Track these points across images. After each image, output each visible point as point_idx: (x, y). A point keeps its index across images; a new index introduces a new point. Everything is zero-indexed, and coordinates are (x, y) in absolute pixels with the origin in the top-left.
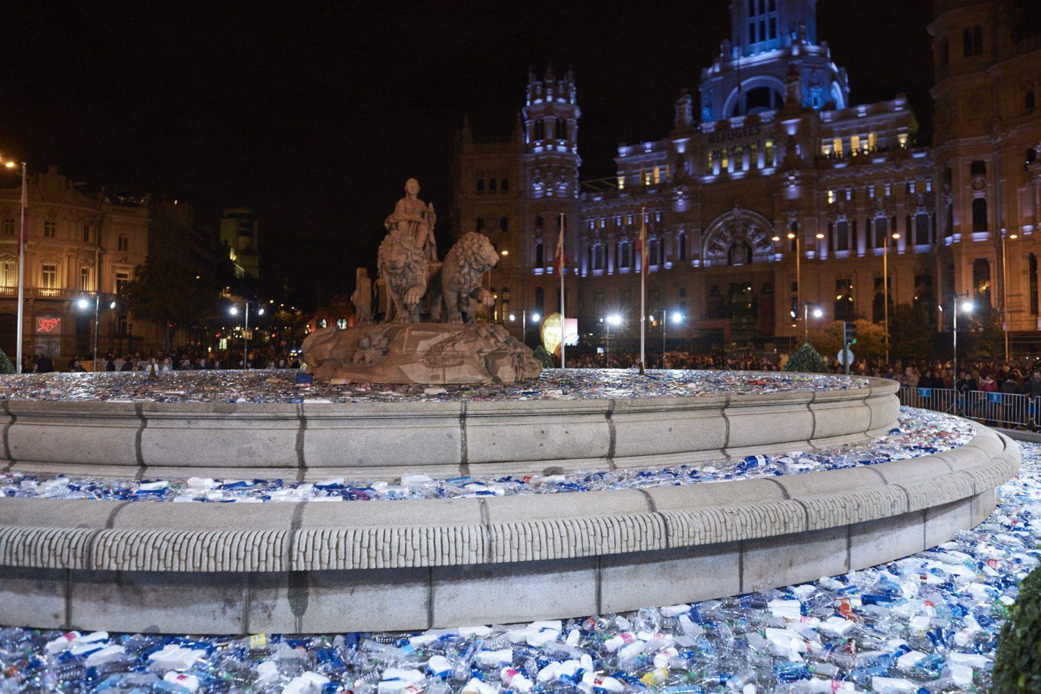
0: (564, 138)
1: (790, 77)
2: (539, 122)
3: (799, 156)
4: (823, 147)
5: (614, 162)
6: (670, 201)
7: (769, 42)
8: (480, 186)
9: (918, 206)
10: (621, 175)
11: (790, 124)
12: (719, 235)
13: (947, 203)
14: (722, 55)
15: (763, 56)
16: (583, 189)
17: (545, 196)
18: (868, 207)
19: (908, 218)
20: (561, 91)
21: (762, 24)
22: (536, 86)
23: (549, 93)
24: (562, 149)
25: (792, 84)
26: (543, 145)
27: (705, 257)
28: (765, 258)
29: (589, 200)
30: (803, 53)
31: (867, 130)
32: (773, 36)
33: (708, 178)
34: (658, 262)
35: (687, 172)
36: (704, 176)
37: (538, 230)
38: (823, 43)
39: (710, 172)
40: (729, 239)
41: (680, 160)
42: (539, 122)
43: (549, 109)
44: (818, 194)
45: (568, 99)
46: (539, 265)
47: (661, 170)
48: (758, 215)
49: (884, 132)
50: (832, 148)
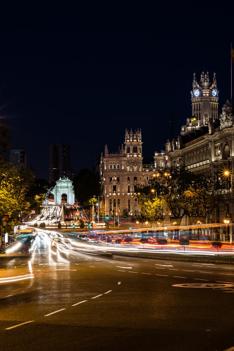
10: (155, 162)
16: (144, 167)
20: (135, 137)
23: (131, 138)
24: (135, 156)
26: (130, 155)
29: (145, 171)
37: (128, 181)
45: (137, 139)
46: (129, 192)
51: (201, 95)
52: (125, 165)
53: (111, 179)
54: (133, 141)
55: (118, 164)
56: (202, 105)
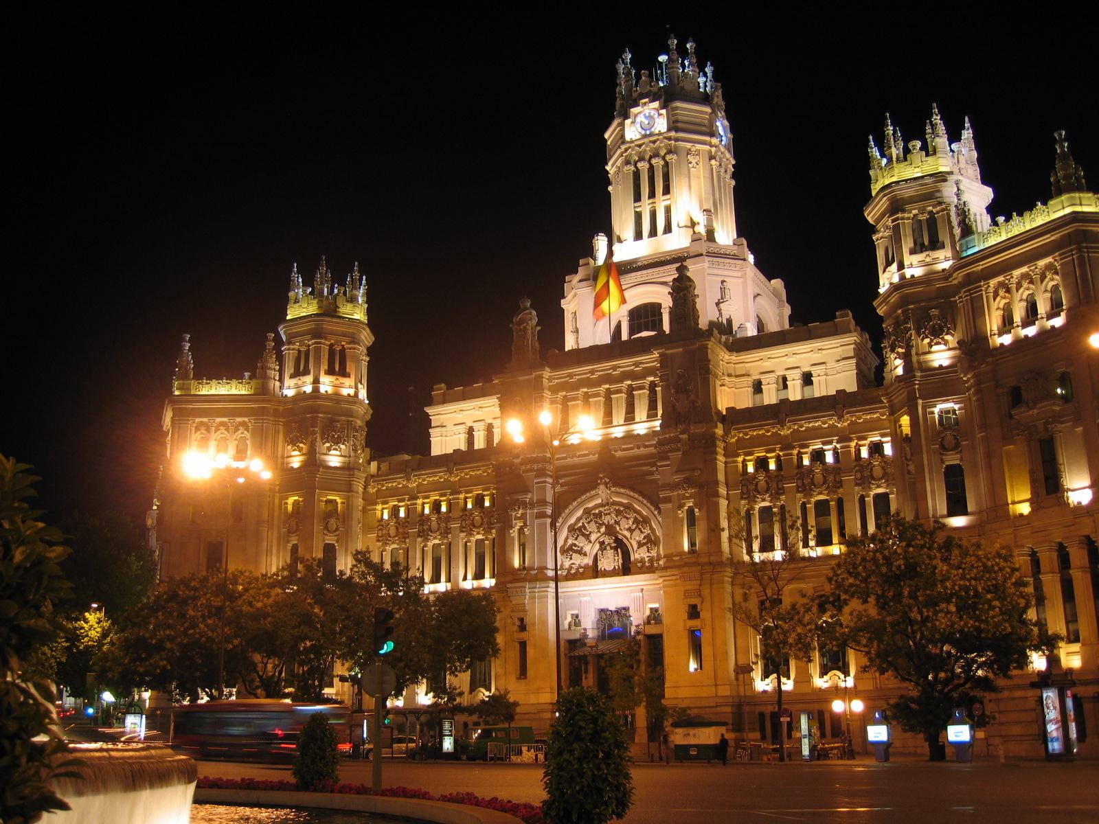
2: (303, 349)
9: (874, 479)
18: (800, 484)
40: (593, 537)
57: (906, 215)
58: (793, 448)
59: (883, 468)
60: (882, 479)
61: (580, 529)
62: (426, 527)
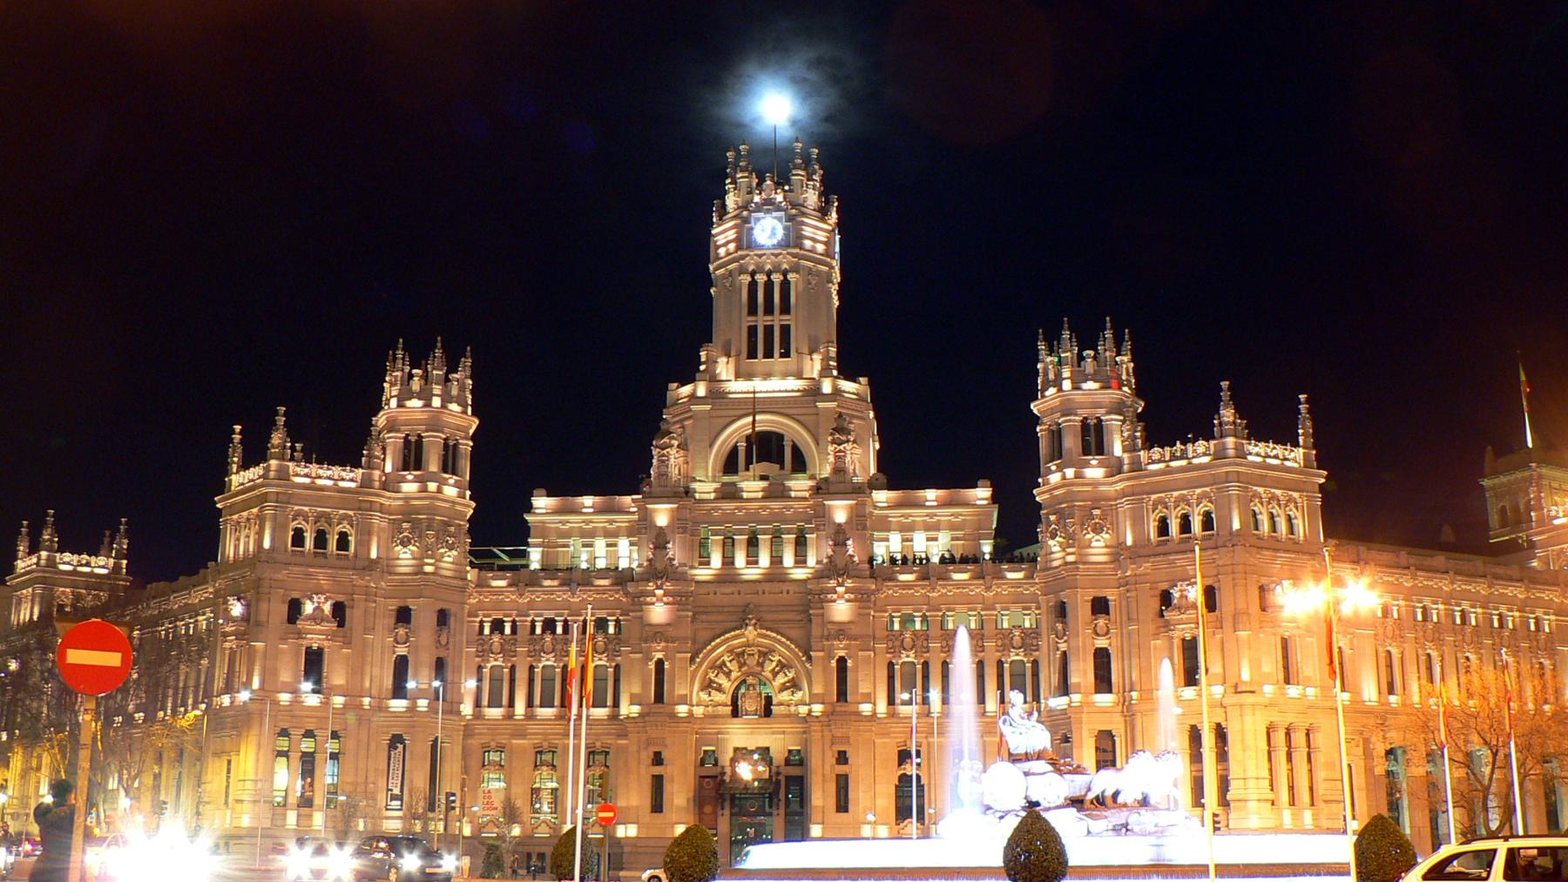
0: (454, 473)
1: (837, 436)
2: (413, 439)
3: (851, 556)
4: (876, 544)
5: (526, 521)
6: (638, 603)
7: (777, 362)
8: (298, 538)
11: (837, 507)
12: (720, 667)
13: (1058, 649)
14: (702, 367)
15: (778, 385)
17: (419, 571)
18: (944, 644)
19: (1000, 664)
20: (454, 392)
21: (769, 330)
22: (411, 376)
24: (450, 491)
25: (841, 447)
26: (422, 481)
27: (694, 702)
28: (793, 709)
29: (481, 584)
30: (837, 393)
31: (936, 527)
32: (786, 354)
33: (703, 574)
34: (609, 703)
35: (672, 560)
36: (692, 567)
37: (401, 631)
38: (863, 380)
39: (706, 563)
40: (734, 675)
41: (660, 541)
42: (413, 439)
43: (434, 425)
44: (874, 617)
46: (399, 691)
47: (608, 545)
48: (784, 640)
49: (959, 533)
50: (888, 547)
51: (793, 239)
52: (381, 534)
53: (295, 608)
54: (444, 406)
55: (339, 529)
56: (800, 288)
57: (1077, 418)
58: (940, 610)
59: (1022, 638)
60: (1020, 648)
61: (720, 667)
62: (537, 648)
